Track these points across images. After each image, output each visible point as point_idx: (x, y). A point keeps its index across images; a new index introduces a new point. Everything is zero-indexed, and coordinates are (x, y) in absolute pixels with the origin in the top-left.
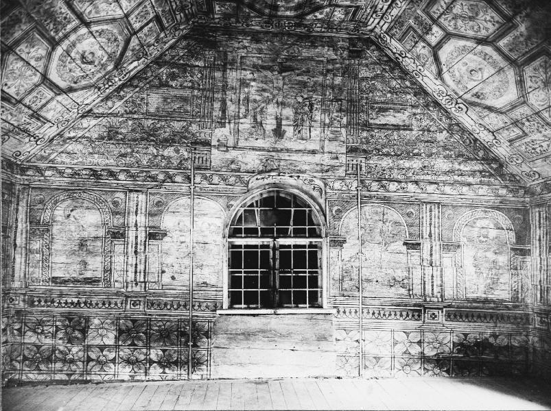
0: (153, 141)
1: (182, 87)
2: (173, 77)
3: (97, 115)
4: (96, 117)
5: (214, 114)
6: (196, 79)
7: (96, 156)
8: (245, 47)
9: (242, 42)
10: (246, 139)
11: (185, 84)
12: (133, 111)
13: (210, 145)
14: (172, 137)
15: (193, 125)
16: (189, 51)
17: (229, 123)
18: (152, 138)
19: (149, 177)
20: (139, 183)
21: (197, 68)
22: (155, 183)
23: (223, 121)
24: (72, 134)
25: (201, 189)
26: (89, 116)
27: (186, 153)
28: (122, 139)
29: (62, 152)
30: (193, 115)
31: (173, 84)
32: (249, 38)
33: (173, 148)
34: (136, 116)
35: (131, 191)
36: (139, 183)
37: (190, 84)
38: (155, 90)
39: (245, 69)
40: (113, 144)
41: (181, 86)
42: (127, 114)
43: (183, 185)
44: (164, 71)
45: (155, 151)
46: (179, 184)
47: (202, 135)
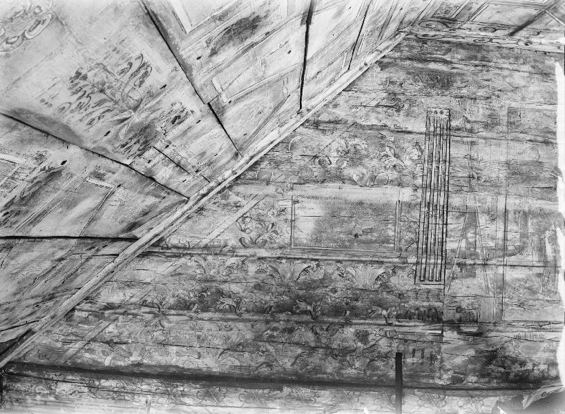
0: (306, 312)
1: (375, 181)
2: (353, 156)
5: (450, 246)
6: (408, 163)
8: (516, 89)
9: (511, 76)
10: (521, 305)
11: (383, 175)
12: (260, 240)
13: (439, 320)
15: (400, 272)
16: (393, 96)
18: (303, 306)
21: (409, 137)
23: (469, 262)
24: (116, 298)
28: (232, 309)
29: (94, 340)
30: (401, 249)
31: (354, 173)
32: (527, 68)
33: (352, 330)
34: (263, 253)
37: (393, 175)
38: (310, 189)
39: (518, 140)
40: (210, 320)
41: (373, 178)
42: (245, 247)
44: (332, 144)
45: (310, 337)
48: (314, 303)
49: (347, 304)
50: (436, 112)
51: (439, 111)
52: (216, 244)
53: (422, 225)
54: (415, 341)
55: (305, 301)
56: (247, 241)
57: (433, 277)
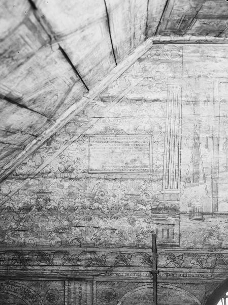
3: (21, 176)
4: (20, 179)
7: (22, 234)
14: (125, 203)
17: (205, 178)
19: (95, 259)
20: (81, 268)
22: (102, 268)
25: (167, 274)
26: (12, 178)
27: (144, 225)
35: (70, 279)
36: (81, 268)
43: (140, 269)
46: (136, 269)
47: (167, 198)
48: (103, 203)
49: (122, 203)
50: (173, 87)
51: (175, 86)
52: (44, 171)
53: (165, 156)
54: (163, 224)
55: (98, 202)
56: (62, 169)
57: (173, 187)
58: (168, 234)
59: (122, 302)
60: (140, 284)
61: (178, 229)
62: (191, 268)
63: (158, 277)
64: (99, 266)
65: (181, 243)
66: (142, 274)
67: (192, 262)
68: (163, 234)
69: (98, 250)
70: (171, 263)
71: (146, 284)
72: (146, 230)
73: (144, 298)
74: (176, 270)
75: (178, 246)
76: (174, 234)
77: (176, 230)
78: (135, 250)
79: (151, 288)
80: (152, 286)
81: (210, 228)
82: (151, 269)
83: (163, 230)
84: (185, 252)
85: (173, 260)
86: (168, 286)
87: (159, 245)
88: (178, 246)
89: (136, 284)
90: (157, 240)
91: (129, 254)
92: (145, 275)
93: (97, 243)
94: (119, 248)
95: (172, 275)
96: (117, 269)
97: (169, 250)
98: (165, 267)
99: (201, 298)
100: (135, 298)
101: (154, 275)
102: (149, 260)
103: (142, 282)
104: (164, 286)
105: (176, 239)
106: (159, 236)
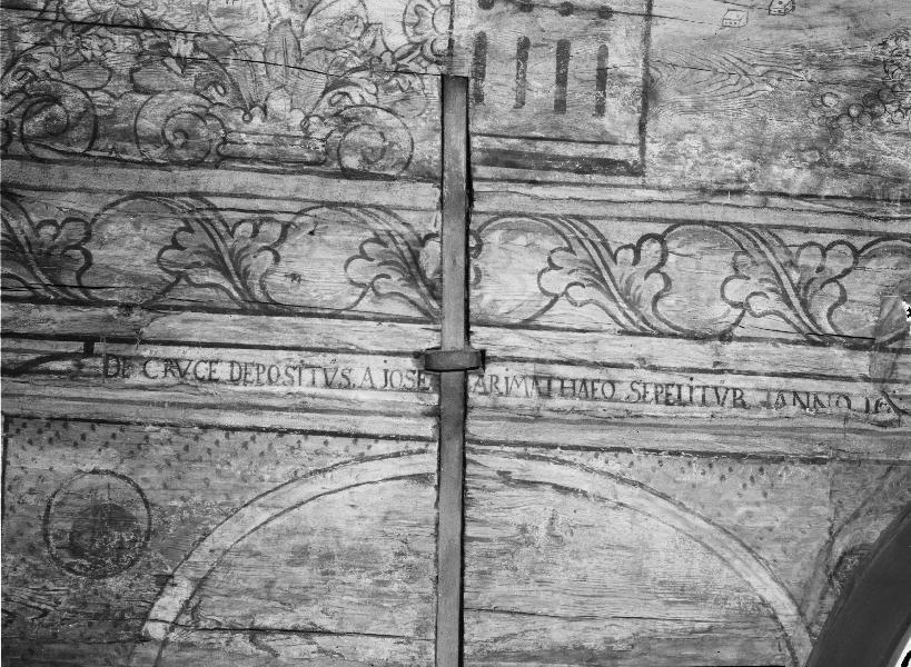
25: (544, 384)
46: (317, 329)
58: (562, 80)
59: (200, 585)
60: (337, 445)
61: (636, 43)
62: (725, 337)
63: (475, 398)
64: (38, 300)
65: (653, 149)
66: (358, 376)
67: (736, 290)
68: (522, 76)
69: (33, 174)
70: (579, 294)
71: (382, 447)
72: (397, 40)
73: (362, 558)
74: (617, 348)
75: (635, 170)
76: (602, 77)
77: (623, 54)
78: (312, 187)
79: (422, 478)
80: (428, 463)
81: (869, 50)
82: (423, 338)
83: (524, 45)
84: (680, 212)
85: (597, 276)
86: (540, 471)
87: (493, 159)
88: (635, 170)
89: (314, 443)
90: (480, 124)
91: (265, 217)
92: (379, 380)
93: (33, 126)
94: (195, 164)
95: (585, 388)
96: (173, 324)
97: (560, 196)
98: (526, 325)
99: (798, 572)
100: (300, 556)
101: (450, 377)
102: (411, 268)
103: (357, 436)
104: (516, 467)
105: (619, 115)
106: (498, 86)
